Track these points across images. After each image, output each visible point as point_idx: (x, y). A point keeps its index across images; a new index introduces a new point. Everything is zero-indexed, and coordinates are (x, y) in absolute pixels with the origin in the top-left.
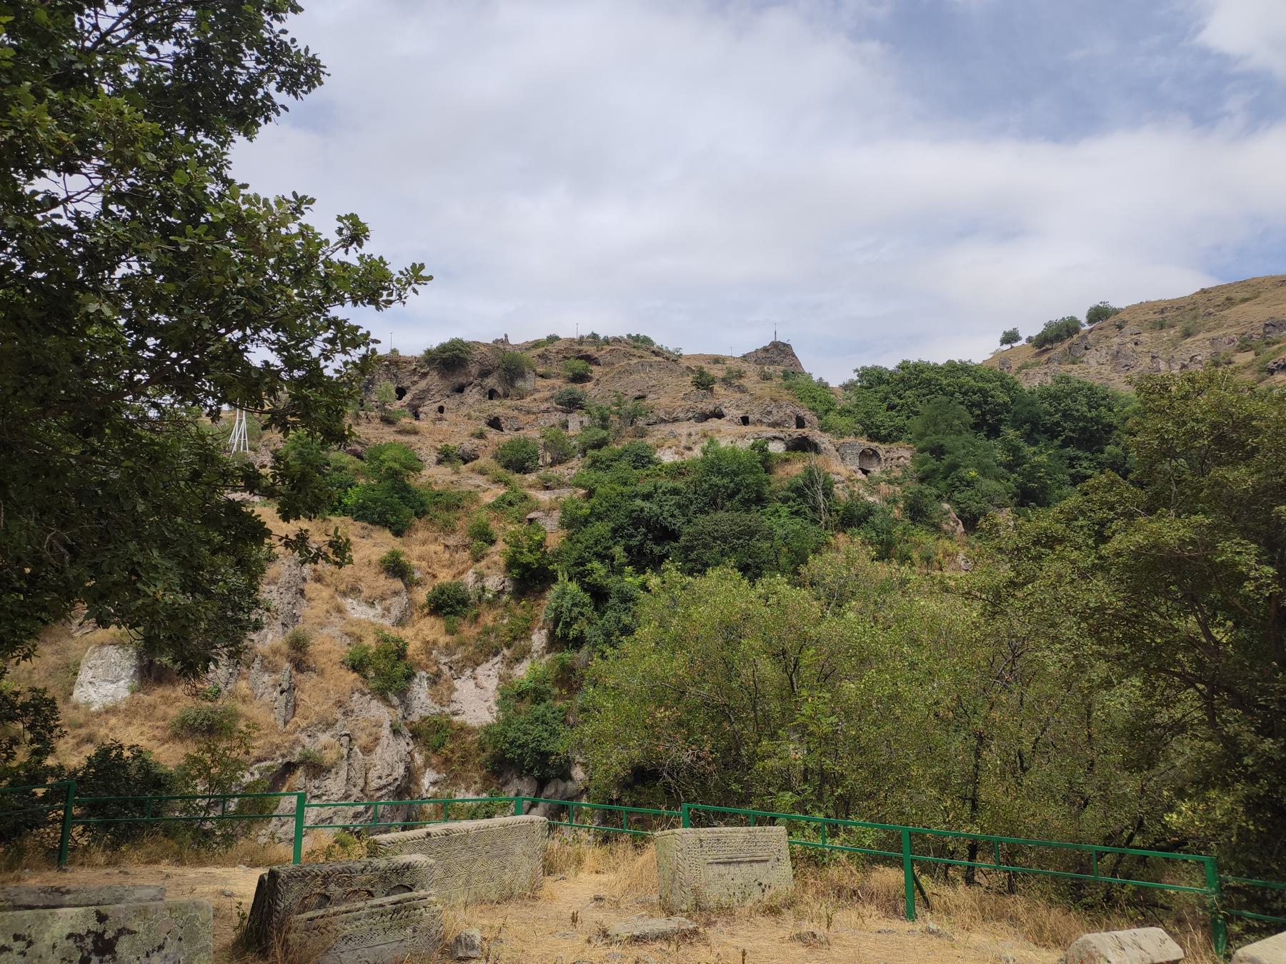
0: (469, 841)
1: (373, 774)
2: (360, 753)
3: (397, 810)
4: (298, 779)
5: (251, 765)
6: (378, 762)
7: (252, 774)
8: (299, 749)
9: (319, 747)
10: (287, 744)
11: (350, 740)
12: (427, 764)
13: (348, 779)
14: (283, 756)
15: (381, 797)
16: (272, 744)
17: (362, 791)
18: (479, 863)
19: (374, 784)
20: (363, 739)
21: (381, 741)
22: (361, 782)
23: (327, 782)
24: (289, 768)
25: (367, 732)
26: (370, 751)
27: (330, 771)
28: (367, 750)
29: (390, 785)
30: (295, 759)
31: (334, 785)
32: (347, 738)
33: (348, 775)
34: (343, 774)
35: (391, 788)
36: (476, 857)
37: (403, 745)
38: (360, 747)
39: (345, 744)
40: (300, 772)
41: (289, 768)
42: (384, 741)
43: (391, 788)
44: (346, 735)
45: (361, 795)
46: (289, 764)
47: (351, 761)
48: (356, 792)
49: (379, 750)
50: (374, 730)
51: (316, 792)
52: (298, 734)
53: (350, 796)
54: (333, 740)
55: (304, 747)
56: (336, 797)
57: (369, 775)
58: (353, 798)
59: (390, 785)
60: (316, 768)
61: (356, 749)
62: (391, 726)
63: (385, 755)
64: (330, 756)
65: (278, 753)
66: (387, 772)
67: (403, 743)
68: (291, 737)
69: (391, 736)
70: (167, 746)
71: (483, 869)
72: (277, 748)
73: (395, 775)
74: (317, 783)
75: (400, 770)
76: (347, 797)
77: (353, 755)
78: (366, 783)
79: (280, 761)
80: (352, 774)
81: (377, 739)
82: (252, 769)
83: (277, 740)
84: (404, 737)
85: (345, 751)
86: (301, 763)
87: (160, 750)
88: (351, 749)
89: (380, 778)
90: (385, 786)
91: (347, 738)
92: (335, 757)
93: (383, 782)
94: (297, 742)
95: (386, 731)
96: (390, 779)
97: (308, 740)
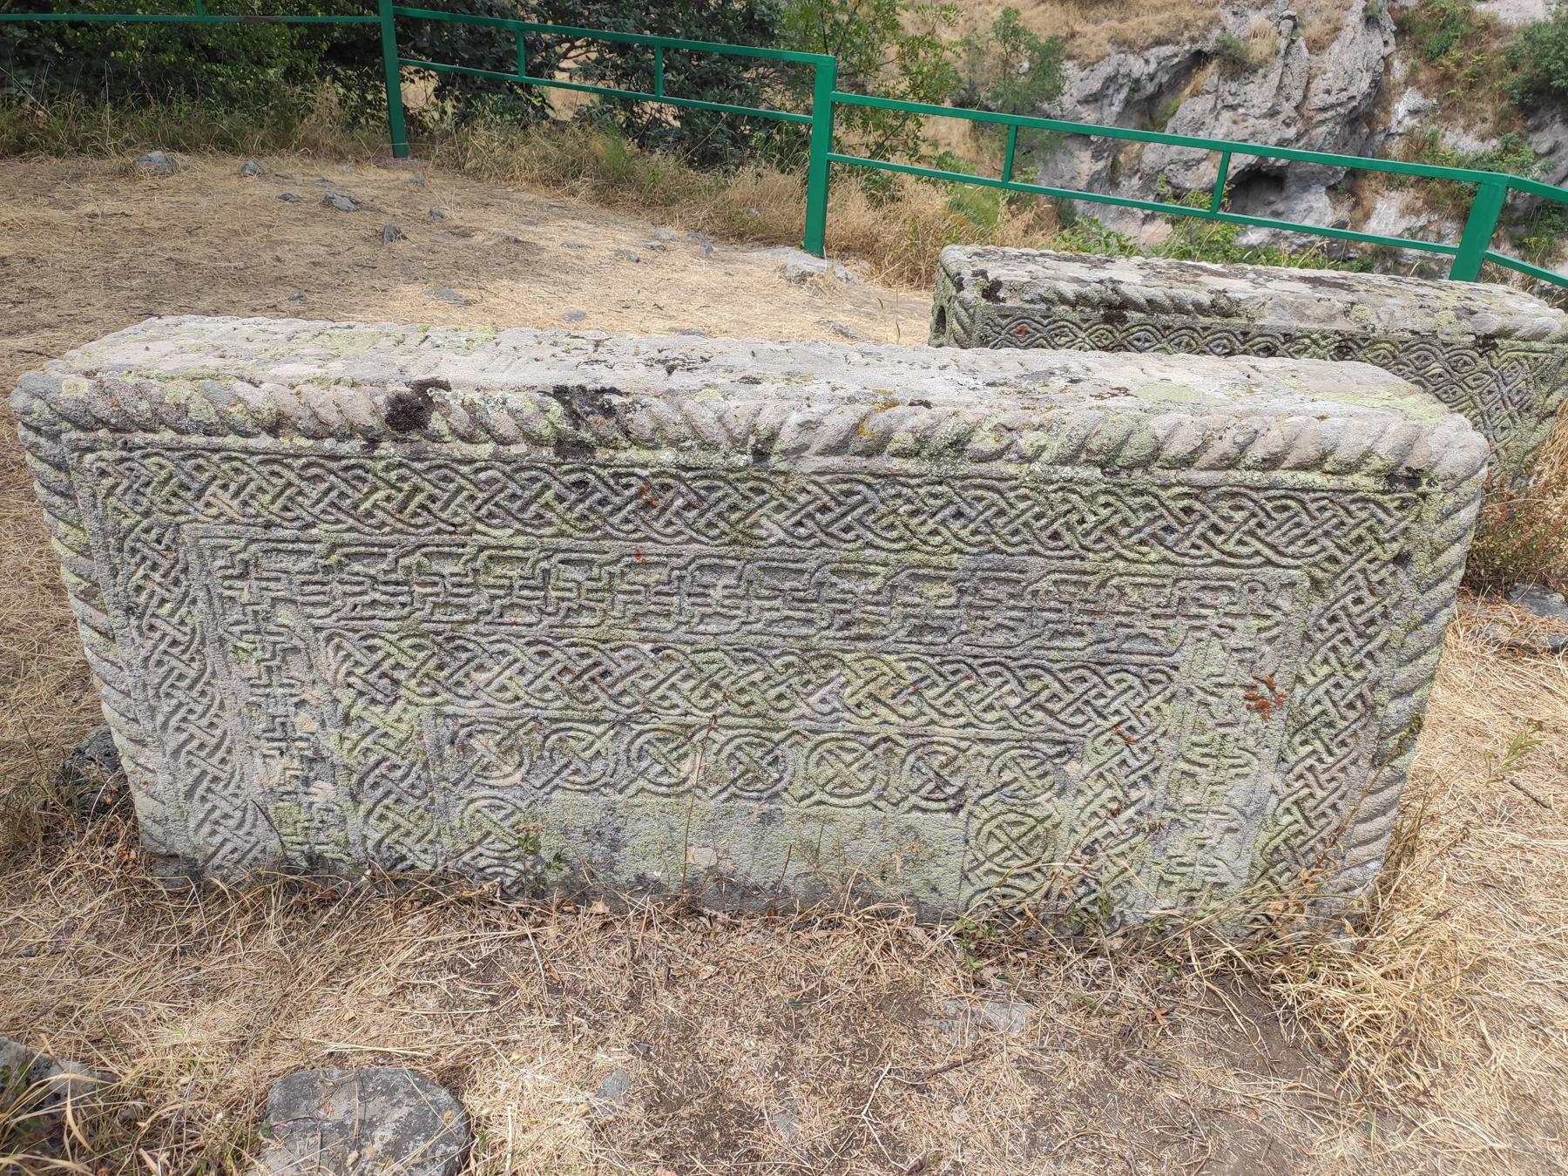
0: (772, 528)
1: (1318, 85)
2: (1305, 51)
3: (1345, 145)
4: (1209, 76)
5: (1147, 48)
6: (1328, 66)
7: (1147, 62)
8: (1217, 32)
9: (1247, 33)
10: (1200, 23)
11: (1295, 27)
12: (1411, 80)
13: (1280, 88)
14: (1193, 40)
15: (1323, 122)
16: (1179, 20)
17: (1297, 108)
18: (849, 680)
19: (1317, 100)
20: (1315, 27)
21: (1343, 33)
22: (1297, 95)
23: (1248, 88)
24: (1199, 59)
25: (1325, 15)
26: (1322, 48)
27: (1255, 71)
28: (1317, 46)
29: (1340, 105)
30: (1208, 47)
31: (1258, 93)
32: (1290, 23)
33: (1281, 81)
34: (1274, 79)
35: (1342, 110)
36: (827, 640)
37: (1377, 44)
38: (1307, 40)
39: (1286, 32)
40: (1212, 68)
41: (1199, 59)
42: (1347, 34)
43: (1342, 110)
44: (1290, 17)
45: (1294, 114)
46: (1199, 53)
47: (1289, 60)
48: (1287, 109)
49: (1336, 47)
50: (1336, 14)
51: (1230, 100)
52: (1218, 9)
53: (1278, 113)
54: (1269, 24)
55: (1224, 29)
56: (1257, 112)
57: (1313, 86)
58: (1281, 117)
59: (1340, 105)
60: (1237, 65)
61: (1301, 42)
62: (1365, 10)
63: (1345, 57)
64: (1259, 49)
65: (1186, 34)
66: (1341, 84)
67: (1378, 41)
68: (1209, 13)
69: (1360, 27)
70: (1043, 7)
71: (885, 721)
72: (1186, 27)
73: (1353, 91)
74: (1234, 86)
75: (1363, 84)
76: (1273, 113)
77: (1294, 51)
78: (1305, 97)
79: (1187, 47)
80: (1286, 81)
81: (1337, 29)
82: (1147, 54)
83: (1187, 14)
84: (1383, 30)
85: (1283, 43)
86: (1216, 53)
87: (1035, 12)
88: (1293, 41)
89: (1328, 92)
90: (1332, 106)
91: (1290, 23)
92: (1266, 50)
93: (1331, 100)
94: (1215, 21)
95: (1354, 18)
96: (1344, 96)
97: (1232, 19)
